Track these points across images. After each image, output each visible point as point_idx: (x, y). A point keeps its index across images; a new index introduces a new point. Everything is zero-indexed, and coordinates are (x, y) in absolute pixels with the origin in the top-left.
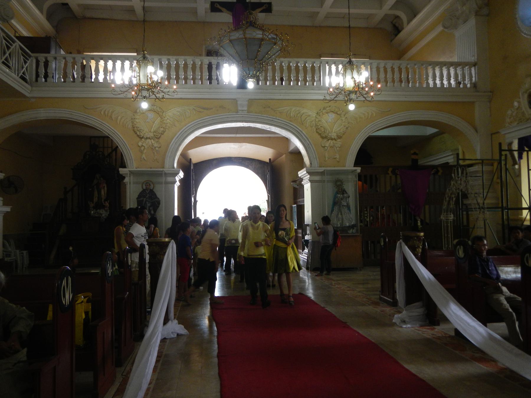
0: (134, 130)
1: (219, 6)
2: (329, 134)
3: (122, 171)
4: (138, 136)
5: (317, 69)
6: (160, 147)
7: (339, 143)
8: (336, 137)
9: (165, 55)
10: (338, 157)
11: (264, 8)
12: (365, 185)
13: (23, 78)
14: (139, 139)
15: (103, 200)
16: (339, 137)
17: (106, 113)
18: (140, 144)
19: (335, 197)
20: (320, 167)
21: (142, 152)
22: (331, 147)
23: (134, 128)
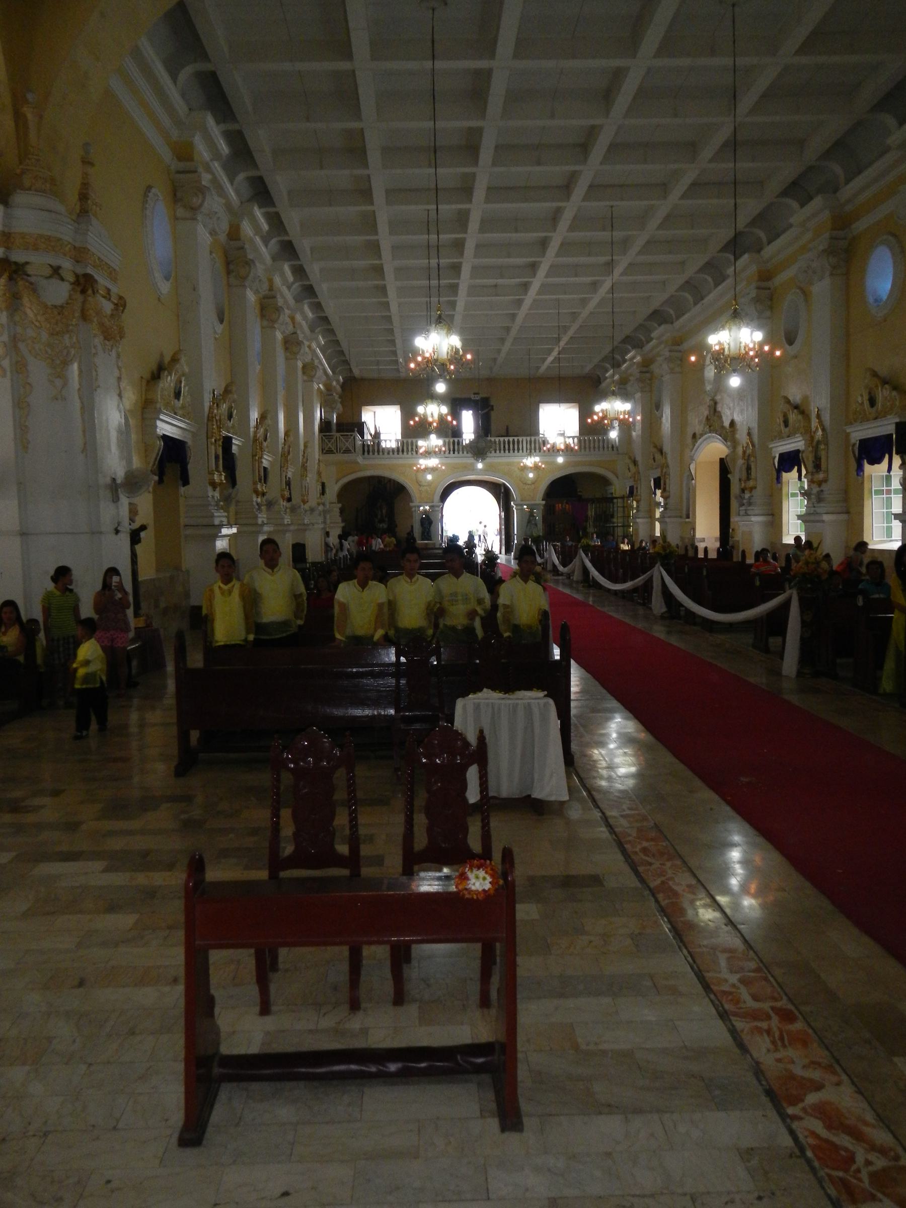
3: (411, 504)
7: (533, 485)
16: (533, 483)
19: (529, 518)
20: (522, 501)
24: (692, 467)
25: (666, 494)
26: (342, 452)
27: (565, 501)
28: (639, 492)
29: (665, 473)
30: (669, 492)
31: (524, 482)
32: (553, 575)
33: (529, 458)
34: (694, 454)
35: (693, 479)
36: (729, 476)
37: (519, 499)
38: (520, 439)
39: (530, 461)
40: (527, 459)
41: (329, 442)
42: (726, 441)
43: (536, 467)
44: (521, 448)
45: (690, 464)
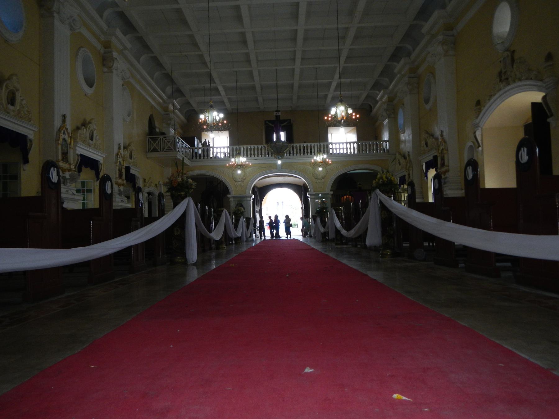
0: (233, 178)
1: (268, 123)
2: (318, 177)
3: (228, 196)
4: (235, 180)
5: (313, 147)
11: (287, 122)
12: (353, 198)
13: (189, 159)
14: (235, 182)
16: (323, 178)
17: (221, 171)
18: (236, 184)
20: (314, 192)
22: (319, 182)
23: (233, 177)
24: (478, 134)
26: (165, 150)
27: (348, 192)
29: (443, 149)
31: (316, 176)
32: (337, 244)
33: (318, 155)
34: (479, 122)
35: (479, 146)
36: (548, 120)
37: (312, 191)
39: (319, 158)
40: (317, 157)
41: (155, 142)
42: (541, 80)
43: (324, 163)
44: (313, 152)
45: (475, 133)
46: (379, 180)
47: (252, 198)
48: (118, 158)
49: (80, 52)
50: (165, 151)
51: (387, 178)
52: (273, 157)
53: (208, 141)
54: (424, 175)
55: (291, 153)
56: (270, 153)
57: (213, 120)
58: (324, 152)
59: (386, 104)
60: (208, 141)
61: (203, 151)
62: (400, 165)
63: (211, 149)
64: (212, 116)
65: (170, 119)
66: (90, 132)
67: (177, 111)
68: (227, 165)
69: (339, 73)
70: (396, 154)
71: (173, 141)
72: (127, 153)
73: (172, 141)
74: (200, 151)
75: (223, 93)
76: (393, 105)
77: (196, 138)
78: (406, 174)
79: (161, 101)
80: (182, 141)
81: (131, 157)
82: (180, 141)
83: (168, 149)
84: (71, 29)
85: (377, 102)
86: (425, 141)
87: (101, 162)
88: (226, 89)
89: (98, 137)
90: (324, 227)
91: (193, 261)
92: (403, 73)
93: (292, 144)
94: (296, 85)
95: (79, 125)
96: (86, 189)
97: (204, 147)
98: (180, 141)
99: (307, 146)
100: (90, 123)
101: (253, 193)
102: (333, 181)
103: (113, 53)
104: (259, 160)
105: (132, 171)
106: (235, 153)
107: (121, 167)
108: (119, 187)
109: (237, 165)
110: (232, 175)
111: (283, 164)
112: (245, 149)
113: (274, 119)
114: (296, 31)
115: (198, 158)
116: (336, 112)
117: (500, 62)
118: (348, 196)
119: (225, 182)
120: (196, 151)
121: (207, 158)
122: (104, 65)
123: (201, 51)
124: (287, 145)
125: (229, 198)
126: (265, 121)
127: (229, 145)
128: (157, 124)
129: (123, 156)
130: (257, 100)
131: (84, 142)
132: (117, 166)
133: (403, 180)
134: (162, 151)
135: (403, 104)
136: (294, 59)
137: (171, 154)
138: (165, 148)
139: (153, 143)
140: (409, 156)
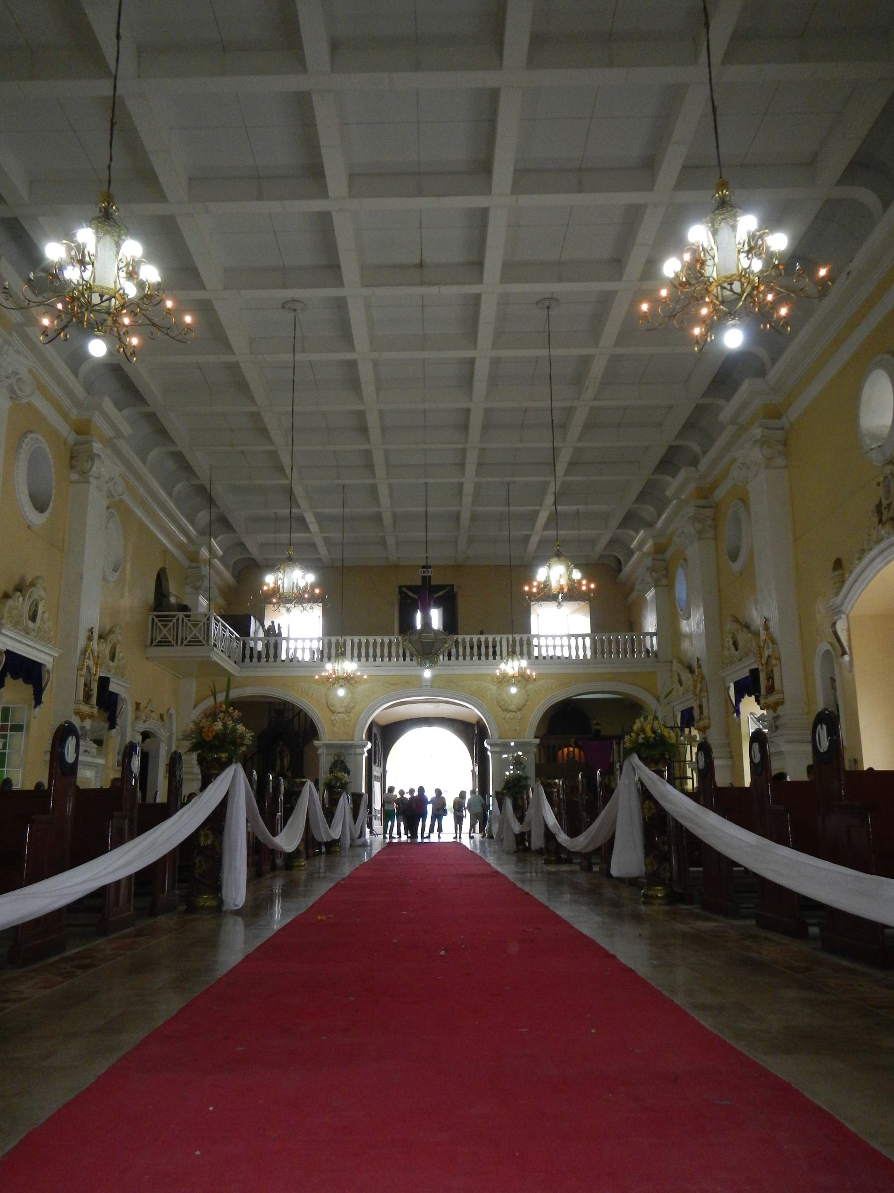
1: (406, 591)
3: (316, 743)
4: (331, 710)
5: (498, 644)
6: (350, 721)
7: (519, 714)
8: (515, 710)
9: (356, 635)
10: (518, 728)
13: (235, 662)
15: (286, 769)
16: (520, 710)
20: (500, 738)
21: (334, 725)
22: (511, 719)
24: (841, 627)
25: (772, 699)
26: (185, 643)
27: (573, 740)
28: (705, 712)
29: (769, 657)
30: (783, 692)
32: (548, 862)
33: (510, 660)
35: (846, 654)
37: (496, 736)
38: (498, 638)
39: (511, 667)
40: (506, 663)
43: (522, 679)
44: (498, 653)
45: (834, 624)
46: (638, 735)
47: (365, 750)
48: (85, 659)
49: (26, 440)
50: (186, 645)
51: (654, 731)
52: (414, 663)
53: (279, 625)
54: (732, 709)
55: (453, 653)
56: (408, 655)
57: (293, 587)
58: (522, 654)
59: (650, 559)
60: (279, 625)
61: (267, 646)
62: (681, 684)
63: (284, 643)
64: (289, 579)
65: (202, 578)
66: (31, 604)
67: (216, 560)
68: (317, 677)
69: (555, 493)
70: (671, 662)
71: (204, 624)
72: (106, 649)
73: (202, 624)
74: (260, 646)
75: (314, 527)
76: (664, 560)
77: (252, 617)
78: (695, 705)
79: (185, 541)
80: (223, 625)
81: (113, 658)
82: (220, 624)
83: (194, 642)
84: (11, 398)
85: (631, 553)
86: (733, 638)
87: (49, 666)
88: (321, 519)
89: (46, 615)
90: (521, 819)
91: (235, 905)
92: (683, 497)
93: (455, 637)
94: (465, 516)
95: (10, 590)
96: (9, 724)
97: (268, 638)
98: (220, 624)
99: (487, 641)
100: (32, 584)
101: (369, 737)
102: (540, 715)
103: (94, 444)
104: (383, 668)
105: (113, 687)
106: (333, 651)
107: (89, 679)
108: (83, 722)
109: (338, 679)
110: (326, 698)
111: (434, 678)
112: (356, 645)
113: (419, 583)
114: (468, 411)
115: (255, 660)
116: (548, 577)
117: (878, 484)
118: (571, 749)
119: (311, 714)
120: (252, 644)
121: (275, 661)
122: (72, 467)
123: (272, 443)
124: (445, 639)
125: (316, 749)
126: (400, 587)
127: (321, 636)
128: (173, 587)
129: (96, 654)
130: (383, 542)
131: (16, 624)
132: (81, 676)
133: (688, 719)
134: (179, 641)
135: (685, 560)
136: (462, 465)
137: (195, 652)
138: (186, 639)
139: (161, 627)
140: (699, 667)
